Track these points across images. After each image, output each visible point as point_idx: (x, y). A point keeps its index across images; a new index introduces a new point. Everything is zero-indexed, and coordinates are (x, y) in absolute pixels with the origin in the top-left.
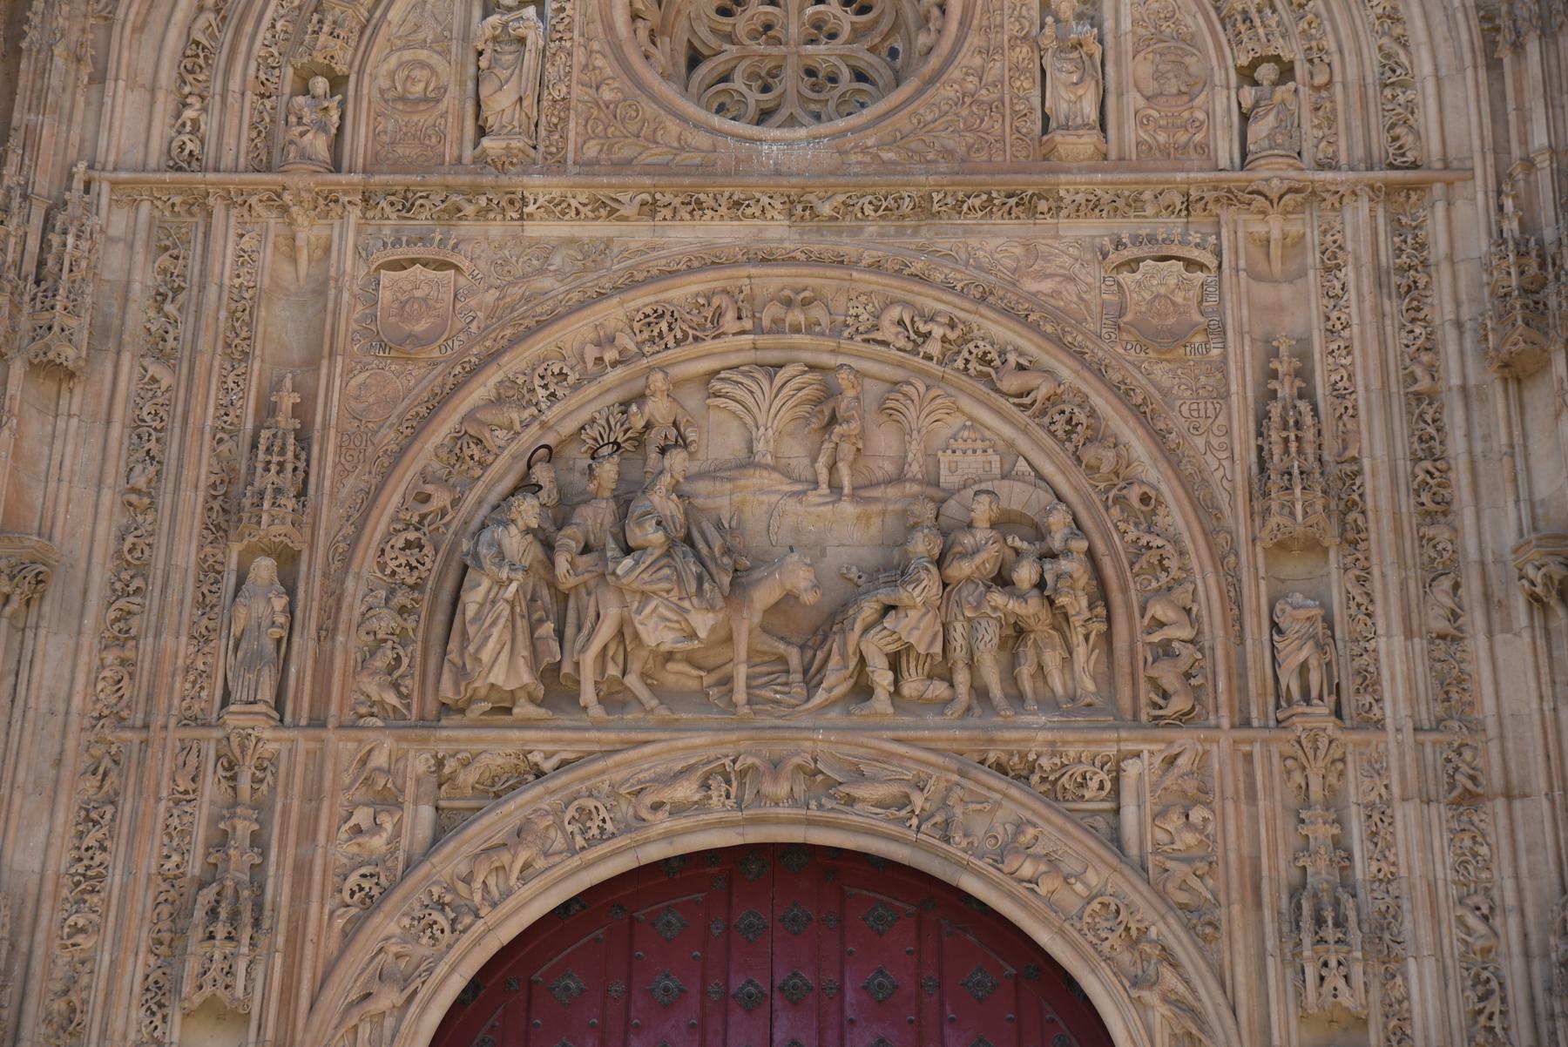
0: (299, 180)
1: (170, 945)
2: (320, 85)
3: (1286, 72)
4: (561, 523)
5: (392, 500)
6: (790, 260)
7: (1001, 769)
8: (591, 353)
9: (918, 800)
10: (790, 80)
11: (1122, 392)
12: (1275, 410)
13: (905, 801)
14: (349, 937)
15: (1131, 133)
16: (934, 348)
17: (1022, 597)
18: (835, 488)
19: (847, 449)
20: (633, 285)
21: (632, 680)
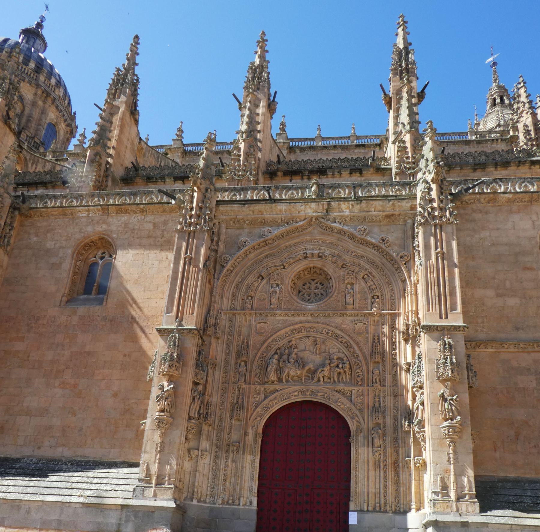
0: (247, 312)
1: (232, 411)
2: (250, 298)
3: (378, 297)
4: (281, 358)
5: (259, 354)
6: (311, 322)
7: (337, 391)
8: (285, 335)
9: (326, 395)
10: (312, 295)
11: (354, 341)
12: (374, 344)
13: (324, 395)
14: (254, 410)
15: (357, 305)
16: (330, 335)
17: (340, 369)
18: (316, 353)
19: (318, 349)
20: (290, 325)
21: (290, 379)
